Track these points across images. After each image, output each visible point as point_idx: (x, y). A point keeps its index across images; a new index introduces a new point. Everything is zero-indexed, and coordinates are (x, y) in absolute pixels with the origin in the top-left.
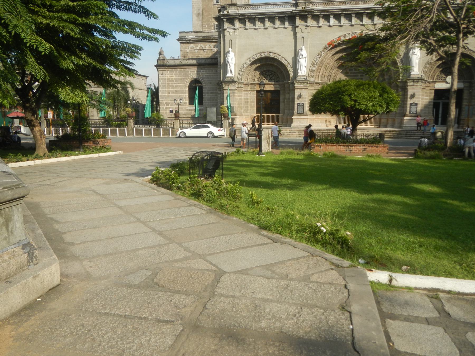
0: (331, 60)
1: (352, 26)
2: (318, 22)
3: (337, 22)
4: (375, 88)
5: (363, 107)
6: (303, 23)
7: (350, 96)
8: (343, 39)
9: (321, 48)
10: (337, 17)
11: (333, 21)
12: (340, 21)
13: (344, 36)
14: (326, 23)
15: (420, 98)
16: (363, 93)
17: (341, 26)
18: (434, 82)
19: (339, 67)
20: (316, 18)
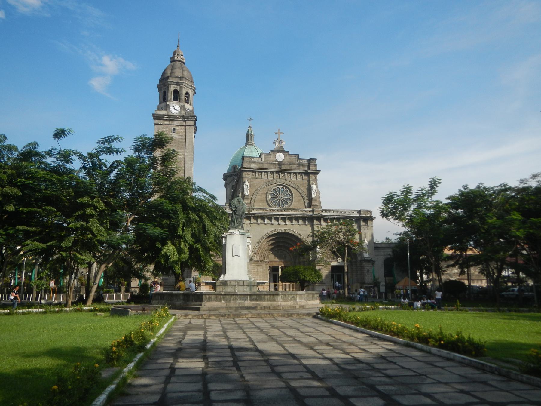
0: (266, 245)
1: (279, 224)
2: (258, 221)
3: (269, 222)
4: (312, 269)
5: (308, 279)
6: (248, 221)
7: (302, 274)
8: (274, 232)
9: (260, 238)
10: (270, 219)
11: (267, 221)
12: (271, 221)
13: (275, 231)
14: (262, 222)
15: (325, 272)
16: (307, 273)
17: (272, 224)
18: (331, 262)
19: (271, 250)
20: (256, 218)
